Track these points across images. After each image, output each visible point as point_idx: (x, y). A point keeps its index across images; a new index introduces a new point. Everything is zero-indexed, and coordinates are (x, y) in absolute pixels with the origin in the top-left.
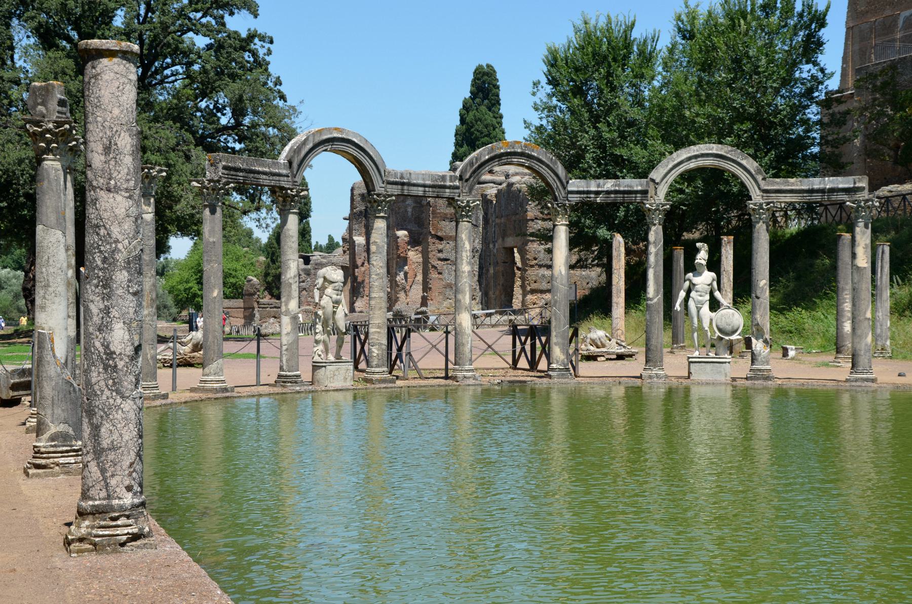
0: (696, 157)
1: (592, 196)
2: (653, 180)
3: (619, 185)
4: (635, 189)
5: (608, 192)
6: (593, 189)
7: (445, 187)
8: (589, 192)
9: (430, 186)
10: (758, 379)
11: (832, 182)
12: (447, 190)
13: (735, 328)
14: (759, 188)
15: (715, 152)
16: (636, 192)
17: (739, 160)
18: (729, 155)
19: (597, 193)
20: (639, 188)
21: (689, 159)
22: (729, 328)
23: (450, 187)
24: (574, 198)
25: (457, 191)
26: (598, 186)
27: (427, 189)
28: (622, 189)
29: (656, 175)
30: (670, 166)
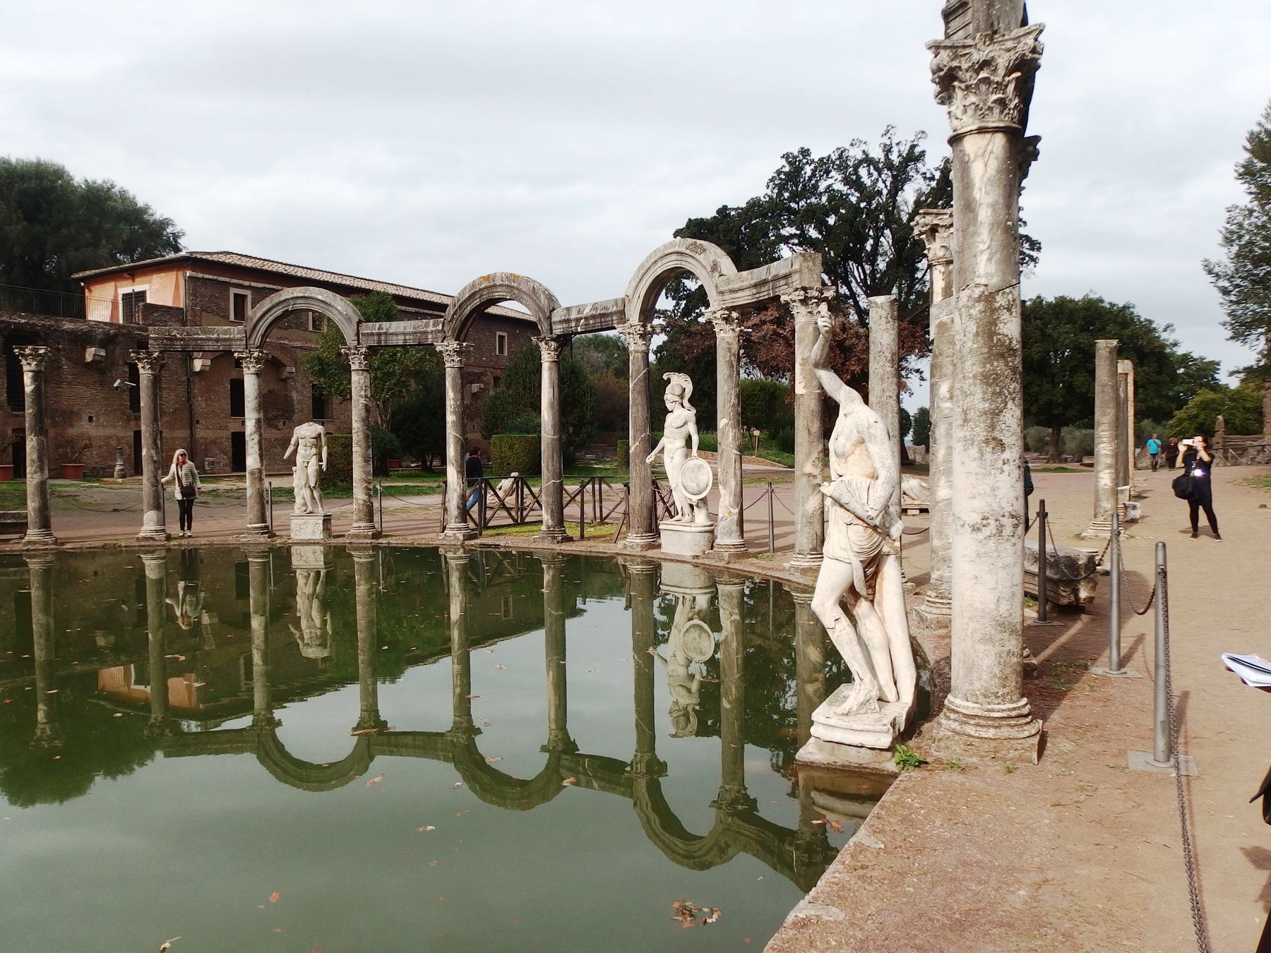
7: (426, 332)
8: (568, 321)
19: (578, 320)
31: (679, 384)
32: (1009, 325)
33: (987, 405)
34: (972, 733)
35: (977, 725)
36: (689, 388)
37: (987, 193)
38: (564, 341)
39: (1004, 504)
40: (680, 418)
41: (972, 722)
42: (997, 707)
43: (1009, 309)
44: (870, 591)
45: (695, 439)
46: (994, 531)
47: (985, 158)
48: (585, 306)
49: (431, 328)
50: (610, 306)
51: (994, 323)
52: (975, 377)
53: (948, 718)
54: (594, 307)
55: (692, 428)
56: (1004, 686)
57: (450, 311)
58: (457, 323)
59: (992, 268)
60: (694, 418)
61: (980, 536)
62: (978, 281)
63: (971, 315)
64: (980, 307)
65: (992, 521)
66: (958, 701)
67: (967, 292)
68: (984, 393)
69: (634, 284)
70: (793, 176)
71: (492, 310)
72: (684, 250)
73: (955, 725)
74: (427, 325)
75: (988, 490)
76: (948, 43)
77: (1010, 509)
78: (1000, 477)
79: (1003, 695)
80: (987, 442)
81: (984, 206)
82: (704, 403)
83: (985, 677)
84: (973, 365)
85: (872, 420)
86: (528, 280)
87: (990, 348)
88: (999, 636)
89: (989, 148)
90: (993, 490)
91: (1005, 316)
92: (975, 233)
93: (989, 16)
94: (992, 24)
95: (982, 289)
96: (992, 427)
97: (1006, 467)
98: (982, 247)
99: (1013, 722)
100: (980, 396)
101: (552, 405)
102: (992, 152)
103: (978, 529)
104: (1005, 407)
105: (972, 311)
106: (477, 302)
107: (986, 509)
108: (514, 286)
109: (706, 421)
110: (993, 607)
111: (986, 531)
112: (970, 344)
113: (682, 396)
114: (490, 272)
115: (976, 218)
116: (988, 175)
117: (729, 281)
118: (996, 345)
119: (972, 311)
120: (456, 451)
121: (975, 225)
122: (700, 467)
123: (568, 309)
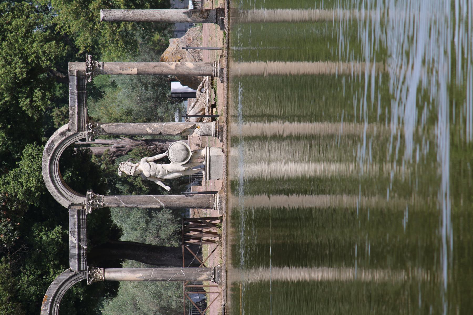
0: (51, 177)
1: (82, 252)
2: (70, 206)
3: (74, 232)
4: (76, 220)
5: (79, 240)
6: (76, 251)
10: (222, 136)
11: (72, 88)
13: (184, 148)
14: (77, 133)
15: (48, 164)
16: (79, 219)
17: (55, 147)
18: (51, 154)
20: (76, 217)
21: (53, 181)
24: (84, 265)
26: (74, 247)
28: (76, 230)
29: (65, 204)
30: (59, 195)
72: (49, 158)
101: (133, 271)
117: (72, 124)
122: (173, 149)
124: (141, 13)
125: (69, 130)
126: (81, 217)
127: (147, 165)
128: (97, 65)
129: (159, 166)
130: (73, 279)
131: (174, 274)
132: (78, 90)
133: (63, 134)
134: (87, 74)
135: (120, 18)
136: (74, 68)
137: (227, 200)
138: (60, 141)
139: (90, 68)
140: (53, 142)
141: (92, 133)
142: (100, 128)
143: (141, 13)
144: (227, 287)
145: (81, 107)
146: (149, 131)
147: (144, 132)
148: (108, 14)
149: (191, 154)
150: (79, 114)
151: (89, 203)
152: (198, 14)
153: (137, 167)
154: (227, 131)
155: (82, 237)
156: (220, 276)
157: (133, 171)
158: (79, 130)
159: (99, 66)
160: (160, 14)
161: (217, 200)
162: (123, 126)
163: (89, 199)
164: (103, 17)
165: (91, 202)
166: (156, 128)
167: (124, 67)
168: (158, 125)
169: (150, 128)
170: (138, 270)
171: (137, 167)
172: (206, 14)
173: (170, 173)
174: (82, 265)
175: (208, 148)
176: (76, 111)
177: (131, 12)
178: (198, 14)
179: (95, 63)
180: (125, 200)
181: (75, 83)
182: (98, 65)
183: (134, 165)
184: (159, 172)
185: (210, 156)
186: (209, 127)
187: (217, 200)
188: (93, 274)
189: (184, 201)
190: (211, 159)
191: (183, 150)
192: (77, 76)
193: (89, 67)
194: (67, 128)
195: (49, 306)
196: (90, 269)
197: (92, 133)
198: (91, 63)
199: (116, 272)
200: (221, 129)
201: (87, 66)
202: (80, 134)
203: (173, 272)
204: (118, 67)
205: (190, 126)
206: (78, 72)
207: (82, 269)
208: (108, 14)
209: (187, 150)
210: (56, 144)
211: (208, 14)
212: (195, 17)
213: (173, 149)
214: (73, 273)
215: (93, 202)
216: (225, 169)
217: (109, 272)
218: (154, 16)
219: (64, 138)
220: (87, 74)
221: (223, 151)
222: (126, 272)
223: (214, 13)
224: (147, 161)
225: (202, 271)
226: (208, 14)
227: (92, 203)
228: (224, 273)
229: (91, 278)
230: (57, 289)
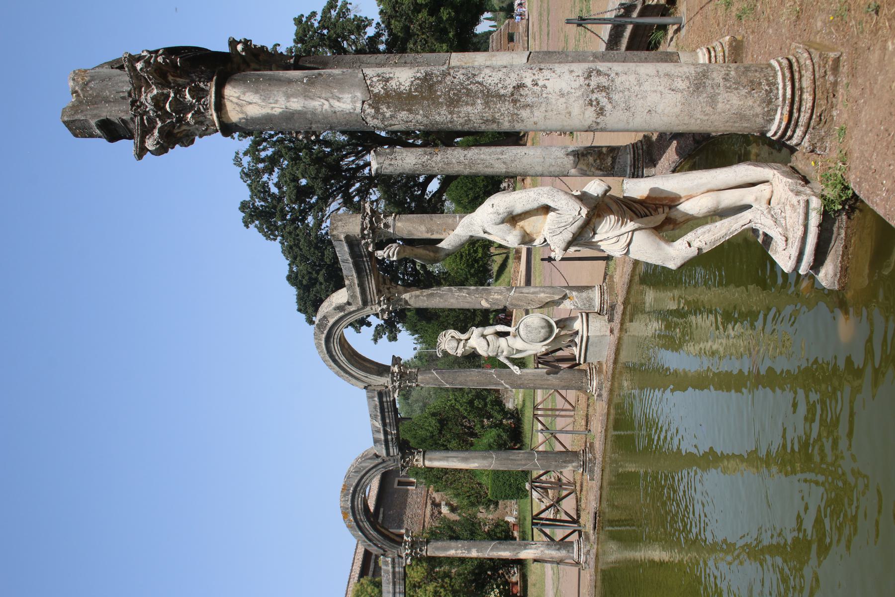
1: (389, 437)
4: (378, 404)
5: (384, 424)
7: (394, 573)
8: (386, 442)
9: (394, 588)
12: (397, 569)
13: (544, 324)
16: (381, 402)
17: (330, 324)
18: (325, 332)
19: (386, 433)
20: (376, 399)
22: (543, 332)
23: (394, 567)
24: (394, 451)
25: (396, 560)
27: (397, 590)
31: (449, 342)
32: (401, 80)
33: (479, 101)
34: (808, 115)
35: (799, 110)
36: (452, 332)
37: (276, 102)
38: (405, 448)
39: (576, 85)
40: (478, 340)
41: (796, 115)
42: (781, 92)
43: (387, 80)
44: (660, 210)
45: (501, 328)
46: (604, 94)
47: (244, 101)
48: (373, 425)
49: (390, 568)
50: (373, 403)
51: (399, 94)
52: (451, 113)
53: (791, 138)
54: (373, 417)
55: (489, 330)
56: (760, 84)
57: (374, 550)
58: (386, 545)
59: (347, 97)
60: (480, 329)
61: (608, 107)
62: (358, 110)
63: (392, 116)
64: (384, 108)
65: (594, 96)
66: (774, 128)
67: (369, 119)
68: (467, 104)
69: (354, 381)
70: (262, 214)
71: (372, 508)
72: (324, 336)
73: (799, 132)
74: (387, 572)
75: (563, 100)
76: (138, 139)
77: (582, 79)
78: (549, 89)
79: (768, 85)
80: (515, 102)
81: (288, 105)
82: (466, 320)
83: (750, 103)
84: (439, 114)
85: (491, 210)
86: (348, 477)
87: (424, 98)
88: (709, 89)
89: (235, 100)
90: (562, 95)
91: (393, 84)
92: (314, 113)
93: (115, 101)
94: (123, 98)
95: (366, 106)
96: (501, 97)
97: (540, 83)
98: (326, 106)
99: (797, 76)
100: (470, 109)
101: (465, 460)
102: (238, 98)
103: (602, 109)
104: (481, 84)
105: (388, 115)
106: (367, 525)
107: (581, 102)
108: (355, 491)
109: (483, 318)
110: (679, 95)
111: (604, 101)
112: (419, 117)
113: (459, 341)
114: (339, 511)
115: (299, 113)
116: (259, 101)
117: (353, 296)
118: (421, 93)
119: (388, 115)
120: (505, 550)
121: (306, 113)
122: (527, 326)
123: (376, 441)
124: (462, 158)
125: (349, 303)
126: (384, 399)
127: (484, 343)
128: (382, 226)
129: (502, 341)
130: (381, 466)
131: (525, 465)
132: (352, 257)
133: (340, 308)
134: (363, 242)
135: (415, 170)
136: (340, 229)
137: (611, 391)
138: (336, 318)
139: (368, 235)
140: (325, 317)
141: (388, 308)
142: (401, 300)
143: (462, 158)
144: (601, 488)
145: (363, 277)
146: (485, 304)
147: (477, 307)
148: (387, 162)
149: (556, 331)
150: (361, 285)
151: (395, 387)
152: (591, 159)
153: (467, 340)
154: (624, 313)
155: (388, 421)
156: (591, 471)
157: (460, 352)
158: (365, 303)
159: (386, 226)
160: (504, 163)
161: (595, 383)
162: (441, 296)
163: (393, 381)
164: (377, 170)
165: (397, 384)
166: (497, 299)
167: (435, 228)
168: (501, 294)
169: (487, 300)
170: (473, 459)
171: (467, 340)
172: (609, 161)
173: (518, 351)
174: (391, 450)
175: (584, 315)
176: (356, 282)
177: (439, 158)
178: (591, 159)
179: (379, 220)
180: (451, 380)
181: (346, 249)
182: (385, 224)
183: (464, 337)
184: (503, 352)
185: (588, 337)
186: (590, 300)
187: (595, 383)
188: (408, 463)
189: (542, 383)
190: (590, 340)
191: (542, 328)
192: (347, 242)
193: (366, 232)
194: (345, 301)
195: (350, 497)
196: (403, 458)
197: (388, 308)
198: (371, 222)
199: (440, 460)
200: (613, 307)
201: (363, 229)
202: (368, 308)
203: (523, 462)
204: (423, 228)
205: (557, 297)
206: (347, 238)
207: (392, 454)
208: (387, 162)
209: (550, 326)
210: (332, 321)
211: (614, 159)
212: (585, 168)
213: (527, 326)
214: (380, 460)
215: (400, 384)
216: (613, 356)
217: (430, 460)
218: (491, 166)
219: (342, 314)
220: (363, 242)
221: (612, 331)
222: (455, 460)
223: (629, 158)
224: (484, 336)
225: (565, 462)
226: (614, 159)
227: (400, 386)
228: (597, 470)
229: (405, 467)
230: (358, 478)
